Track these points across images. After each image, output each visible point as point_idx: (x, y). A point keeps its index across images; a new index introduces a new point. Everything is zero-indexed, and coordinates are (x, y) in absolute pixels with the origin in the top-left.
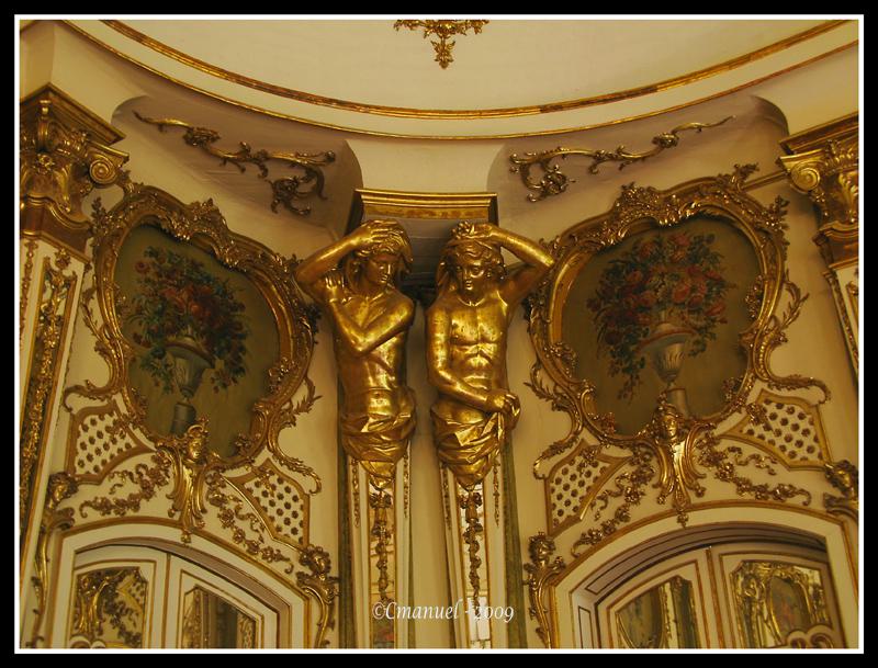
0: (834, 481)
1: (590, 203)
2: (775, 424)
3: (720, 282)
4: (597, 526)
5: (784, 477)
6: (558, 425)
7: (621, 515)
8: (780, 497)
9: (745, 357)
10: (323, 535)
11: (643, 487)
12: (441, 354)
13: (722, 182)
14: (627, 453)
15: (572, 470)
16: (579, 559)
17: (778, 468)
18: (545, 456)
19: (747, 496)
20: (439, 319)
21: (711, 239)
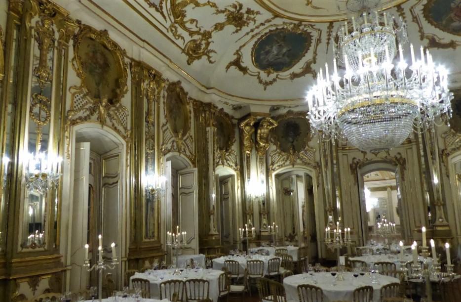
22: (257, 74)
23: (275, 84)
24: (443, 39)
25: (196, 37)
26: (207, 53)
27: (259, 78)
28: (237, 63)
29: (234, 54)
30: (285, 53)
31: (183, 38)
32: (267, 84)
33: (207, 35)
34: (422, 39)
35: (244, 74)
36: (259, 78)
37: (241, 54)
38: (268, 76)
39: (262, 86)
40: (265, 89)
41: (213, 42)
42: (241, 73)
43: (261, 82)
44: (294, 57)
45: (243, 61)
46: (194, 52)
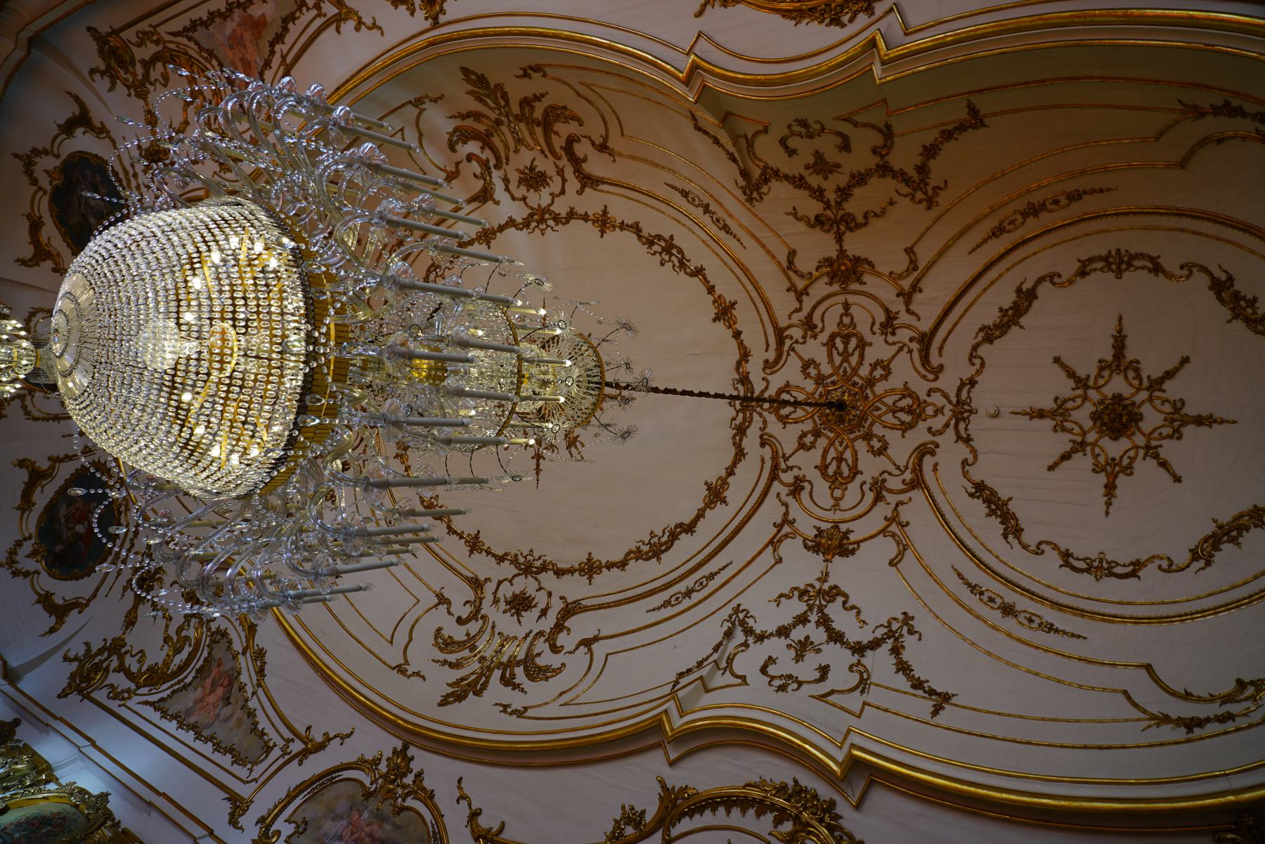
22: (56, 152)
23: (26, 180)
24: (42, 492)
25: (139, 70)
26: (108, 72)
28: (82, 120)
30: (88, 221)
31: (139, 45)
32: (28, 164)
33: (140, 90)
34: (50, 459)
35: (59, 126)
37: (101, 136)
38: (46, 171)
39: (25, 150)
40: (16, 155)
41: (129, 95)
42: (62, 121)
43: (35, 152)
45: (87, 134)
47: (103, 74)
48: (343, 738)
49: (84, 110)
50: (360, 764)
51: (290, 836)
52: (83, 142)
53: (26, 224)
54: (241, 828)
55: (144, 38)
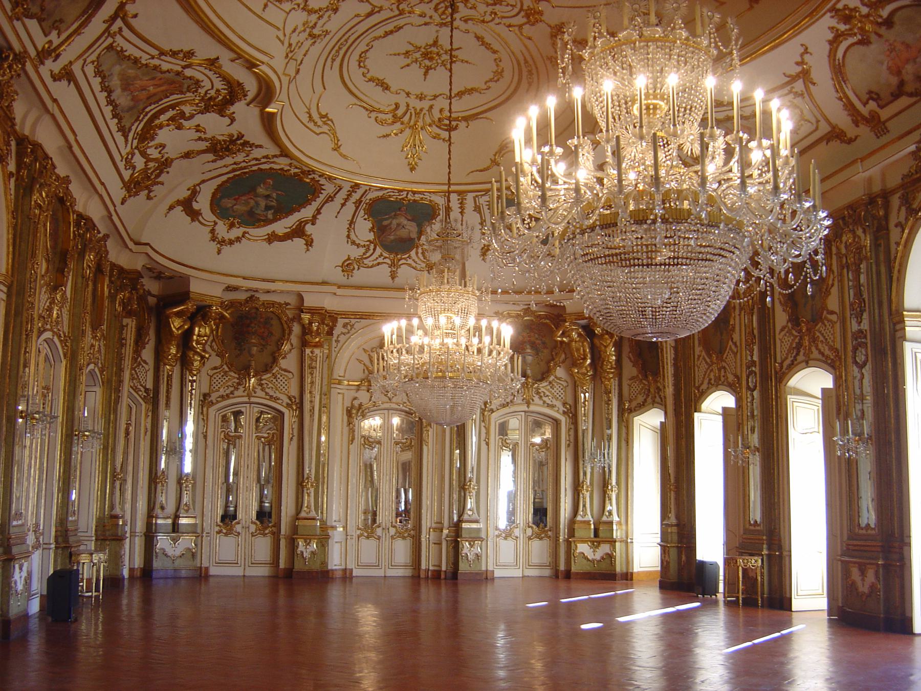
0: (291, 400)
1: (242, 296)
2: (279, 380)
3: (272, 334)
4: (225, 394)
5: (278, 395)
6: (216, 361)
7: (232, 393)
8: (276, 399)
9: (275, 361)
10: (150, 385)
11: (239, 387)
12: (195, 337)
13: (280, 304)
14: (237, 376)
15: (220, 376)
16: (218, 402)
17: (277, 392)
18: (212, 369)
19: (268, 397)
20: (197, 329)
21: (272, 319)
23: (237, 244)
25: (151, 165)
27: (213, 231)
29: (188, 190)
31: (134, 168)
35: (193, 220)
36: (213, 231)
39: (214, 246)
40: (219, 252)
41: (168, 172)
42: (189, 218)
43: (214, 239)
44: (282, 211)
46: (134, 186)
47: (150, 191)
48: (806, 51)
49: (179, 202)
50: (834, 43)
51: (879, 106)
52: (203, 203)
53: (276, 244)
54: (856, 137)
55: (129, 164)
